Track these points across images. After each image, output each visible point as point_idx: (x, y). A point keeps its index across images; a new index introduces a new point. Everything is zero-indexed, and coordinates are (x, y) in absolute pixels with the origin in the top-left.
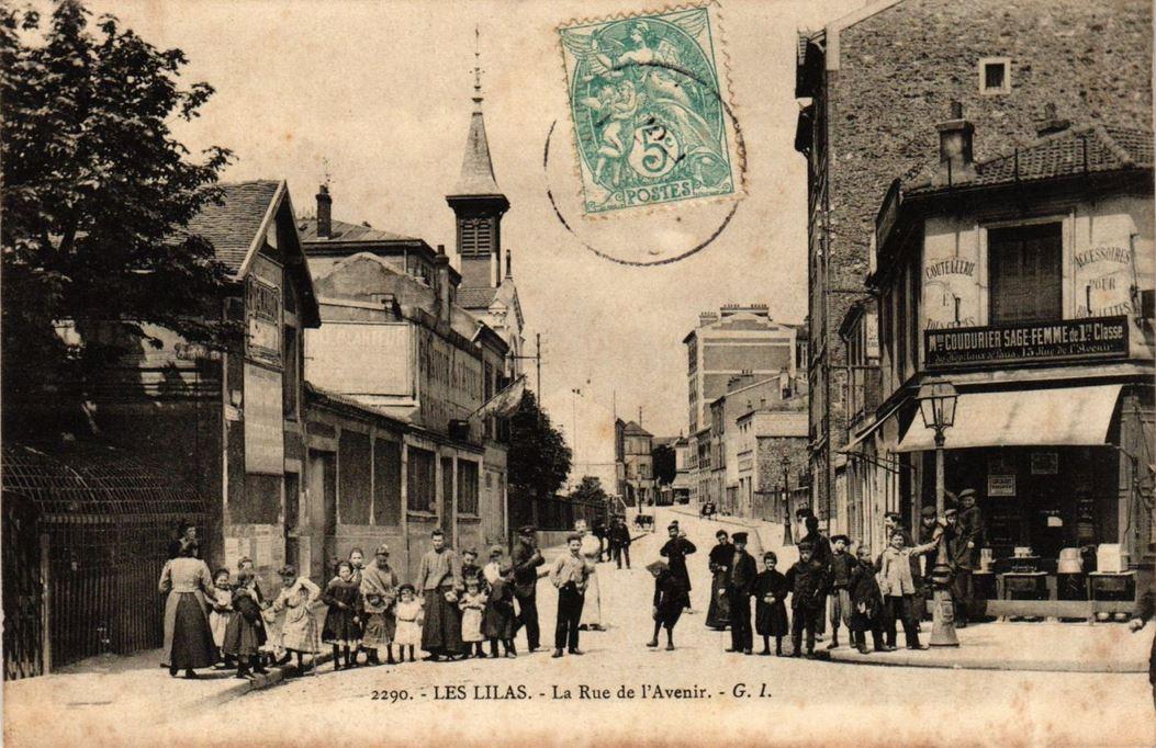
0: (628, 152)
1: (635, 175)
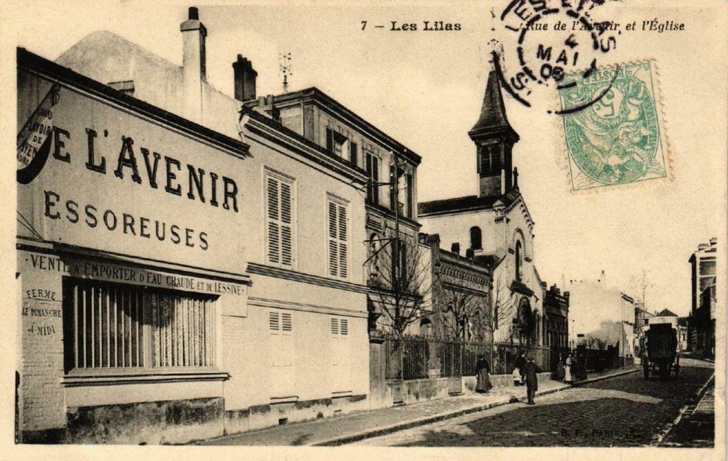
0: (624, 102)
1: (619, 87)
